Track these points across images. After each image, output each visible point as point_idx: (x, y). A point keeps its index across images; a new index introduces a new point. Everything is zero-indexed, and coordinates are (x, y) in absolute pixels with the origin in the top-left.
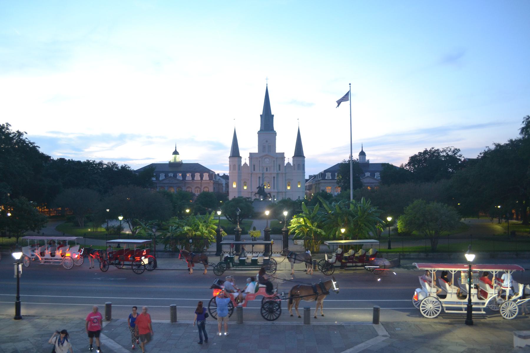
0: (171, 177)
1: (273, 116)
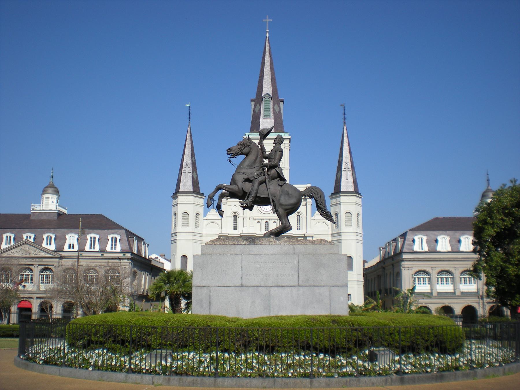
0: (27, 243)
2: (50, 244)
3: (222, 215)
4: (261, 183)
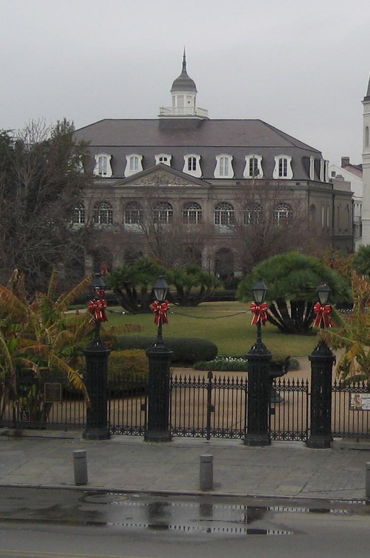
0: (161, 167)
2: (194, 169)
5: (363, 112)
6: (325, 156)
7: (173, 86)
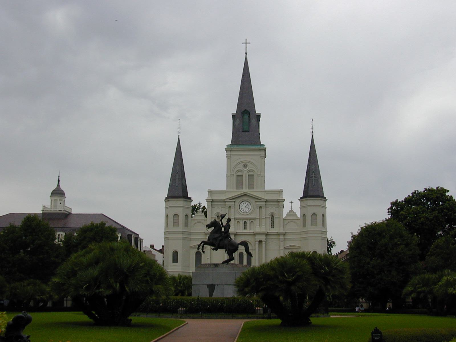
1: (259, 116)
3: (206, 216)
4: (221, 240)
5: (165, 206)
6: (141, 236)
7: (52, 194)
